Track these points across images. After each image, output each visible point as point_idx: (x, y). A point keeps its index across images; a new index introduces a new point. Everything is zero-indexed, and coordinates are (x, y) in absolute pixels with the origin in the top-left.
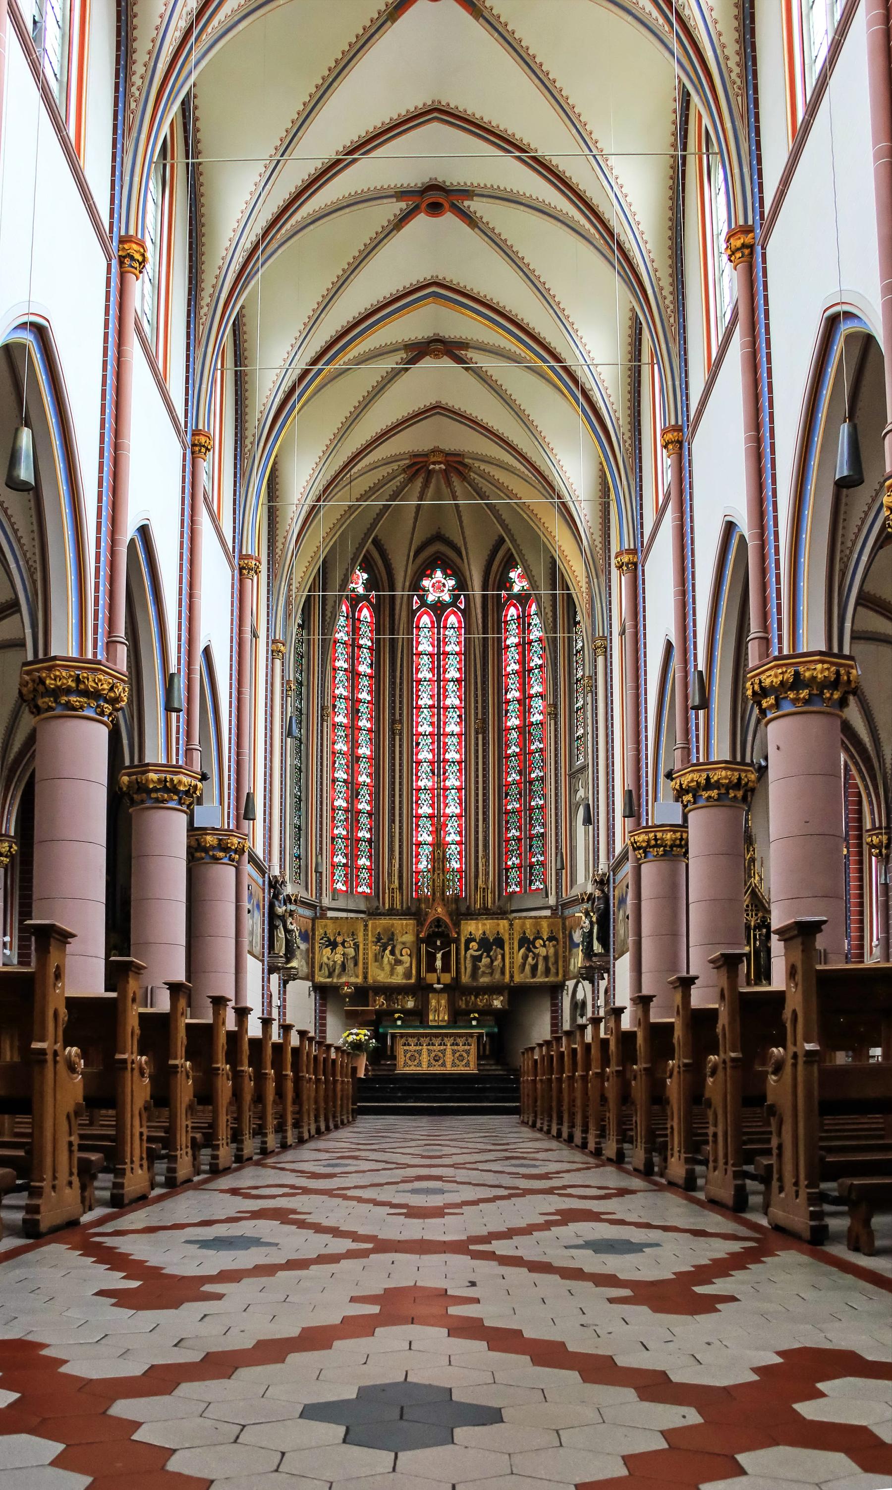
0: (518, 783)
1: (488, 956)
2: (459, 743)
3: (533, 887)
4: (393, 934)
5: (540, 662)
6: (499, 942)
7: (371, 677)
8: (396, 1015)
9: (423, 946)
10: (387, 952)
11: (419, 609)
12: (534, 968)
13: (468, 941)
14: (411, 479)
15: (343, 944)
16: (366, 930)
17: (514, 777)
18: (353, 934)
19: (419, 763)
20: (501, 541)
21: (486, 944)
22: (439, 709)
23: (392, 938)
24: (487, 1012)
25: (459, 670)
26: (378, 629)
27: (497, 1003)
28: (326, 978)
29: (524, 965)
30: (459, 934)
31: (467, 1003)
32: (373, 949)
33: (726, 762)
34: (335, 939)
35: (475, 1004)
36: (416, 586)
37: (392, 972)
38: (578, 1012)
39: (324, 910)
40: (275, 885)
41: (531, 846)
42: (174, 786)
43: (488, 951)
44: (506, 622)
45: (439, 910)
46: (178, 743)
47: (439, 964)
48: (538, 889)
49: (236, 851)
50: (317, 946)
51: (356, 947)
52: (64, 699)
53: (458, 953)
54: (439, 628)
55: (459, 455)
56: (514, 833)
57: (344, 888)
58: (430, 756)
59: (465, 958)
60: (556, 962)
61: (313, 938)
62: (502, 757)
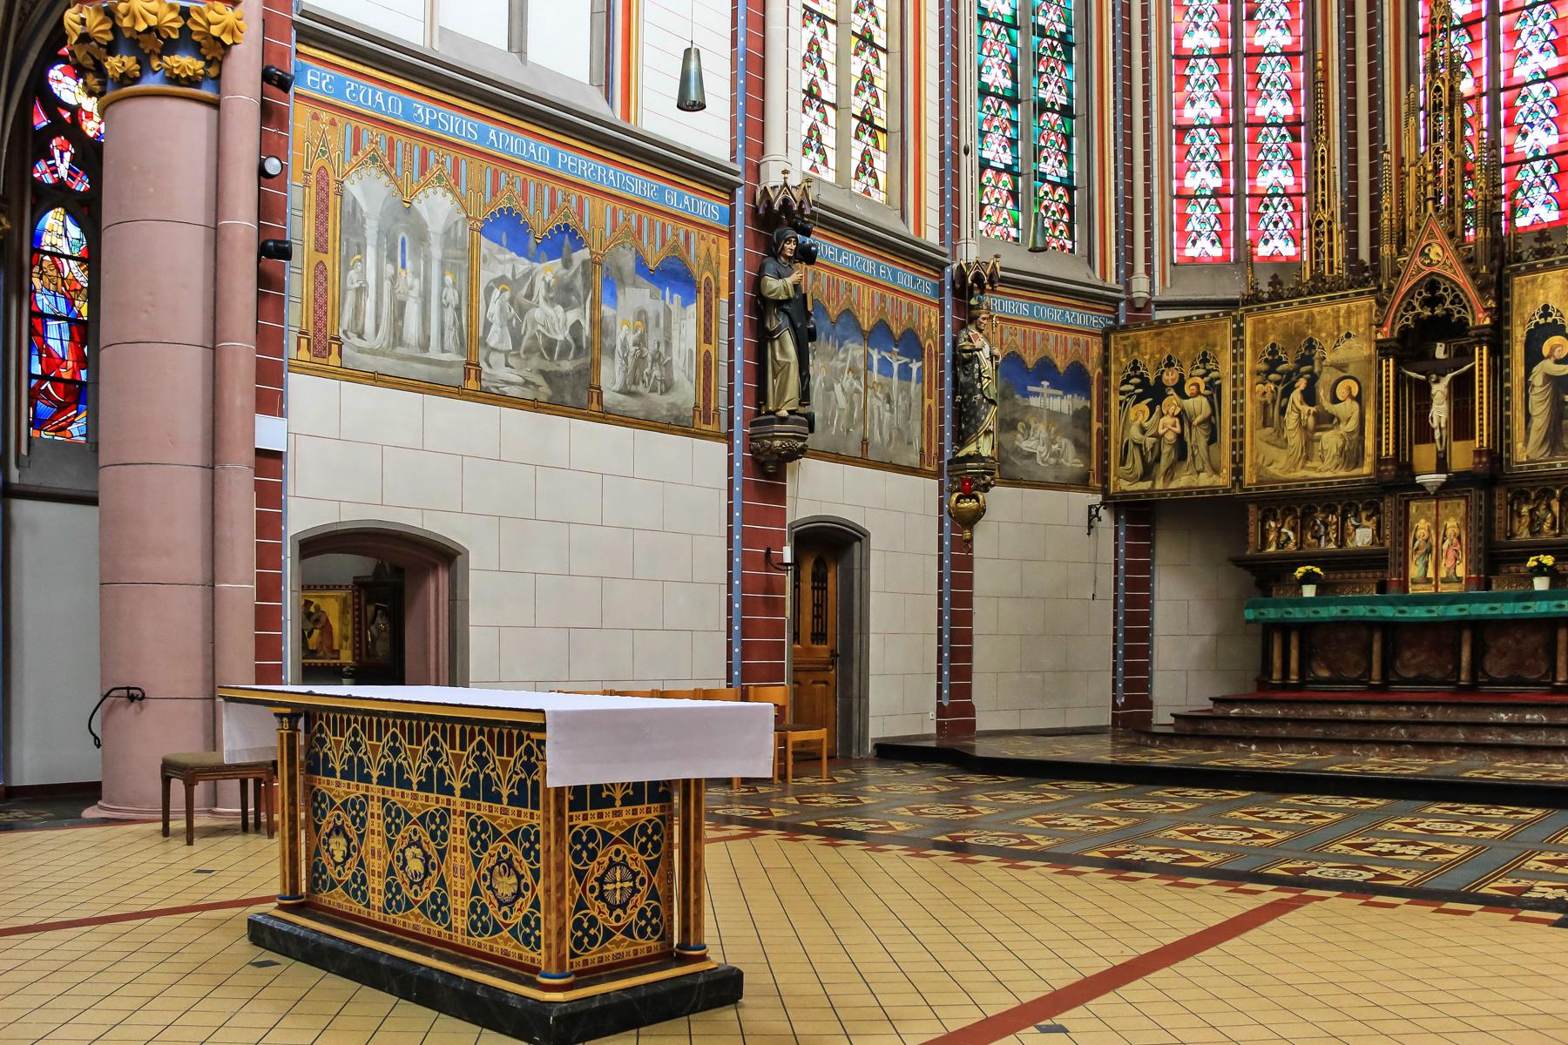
4: (1311, 345)
8: (1300, 572)
10: (1296, 396)
15: (1179, 388)
16: (1238, 343)
18: (1205, 361)
28: (1133, 481)
32: (1256, 391)
34: (1159, 379)
39: (1139, 312)
47: (1439, 412)
50: (1114, 400)
51: (1214, 389)
57: (1217, 251)
59: (1527, 385)
61: (1104, 383)
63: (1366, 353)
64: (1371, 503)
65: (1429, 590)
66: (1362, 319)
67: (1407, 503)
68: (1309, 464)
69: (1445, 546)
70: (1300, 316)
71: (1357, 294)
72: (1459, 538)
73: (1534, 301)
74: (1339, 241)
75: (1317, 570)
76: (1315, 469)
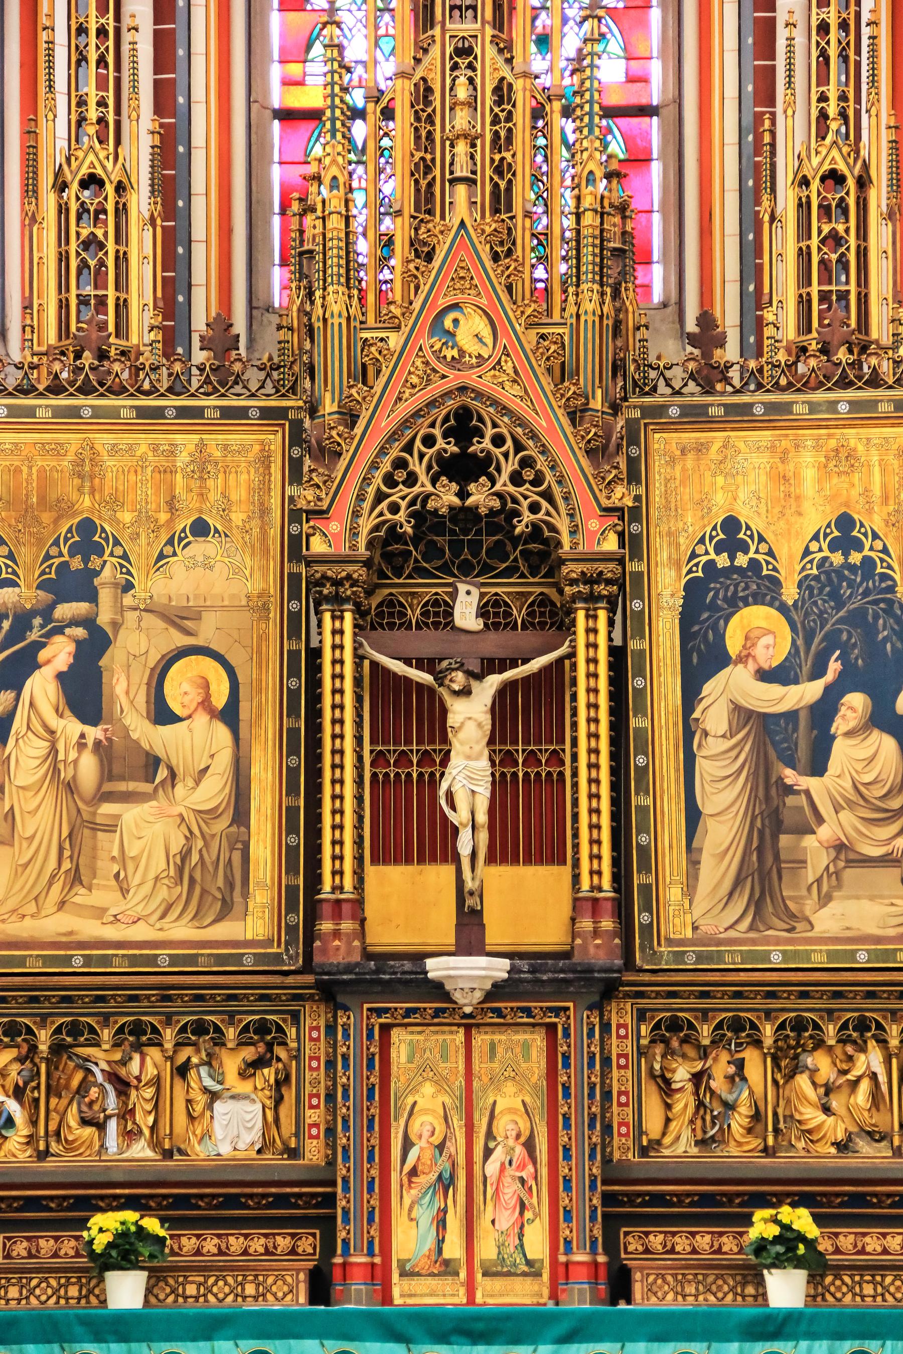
4: (88, 540)
8: (105, 1226)
10: (42, 687)
13: (706, 606)
30: (630, 521)
31: (710, 1111)
45: (471, 330)
47: (468, 779)
59: (689, 731)
63: (254, 586)
64: (262, 1028)
65: (447, 1295)
66: (240, 484)
67: (386, 1029)
68: (81, 896)
69: (492, 1168)
70: (58, 450)
71: (227, 413)
72: (530, 1145)
73: (703, 504)
74: (142, 244)
75: (152, 1225)
76: (99, 912)
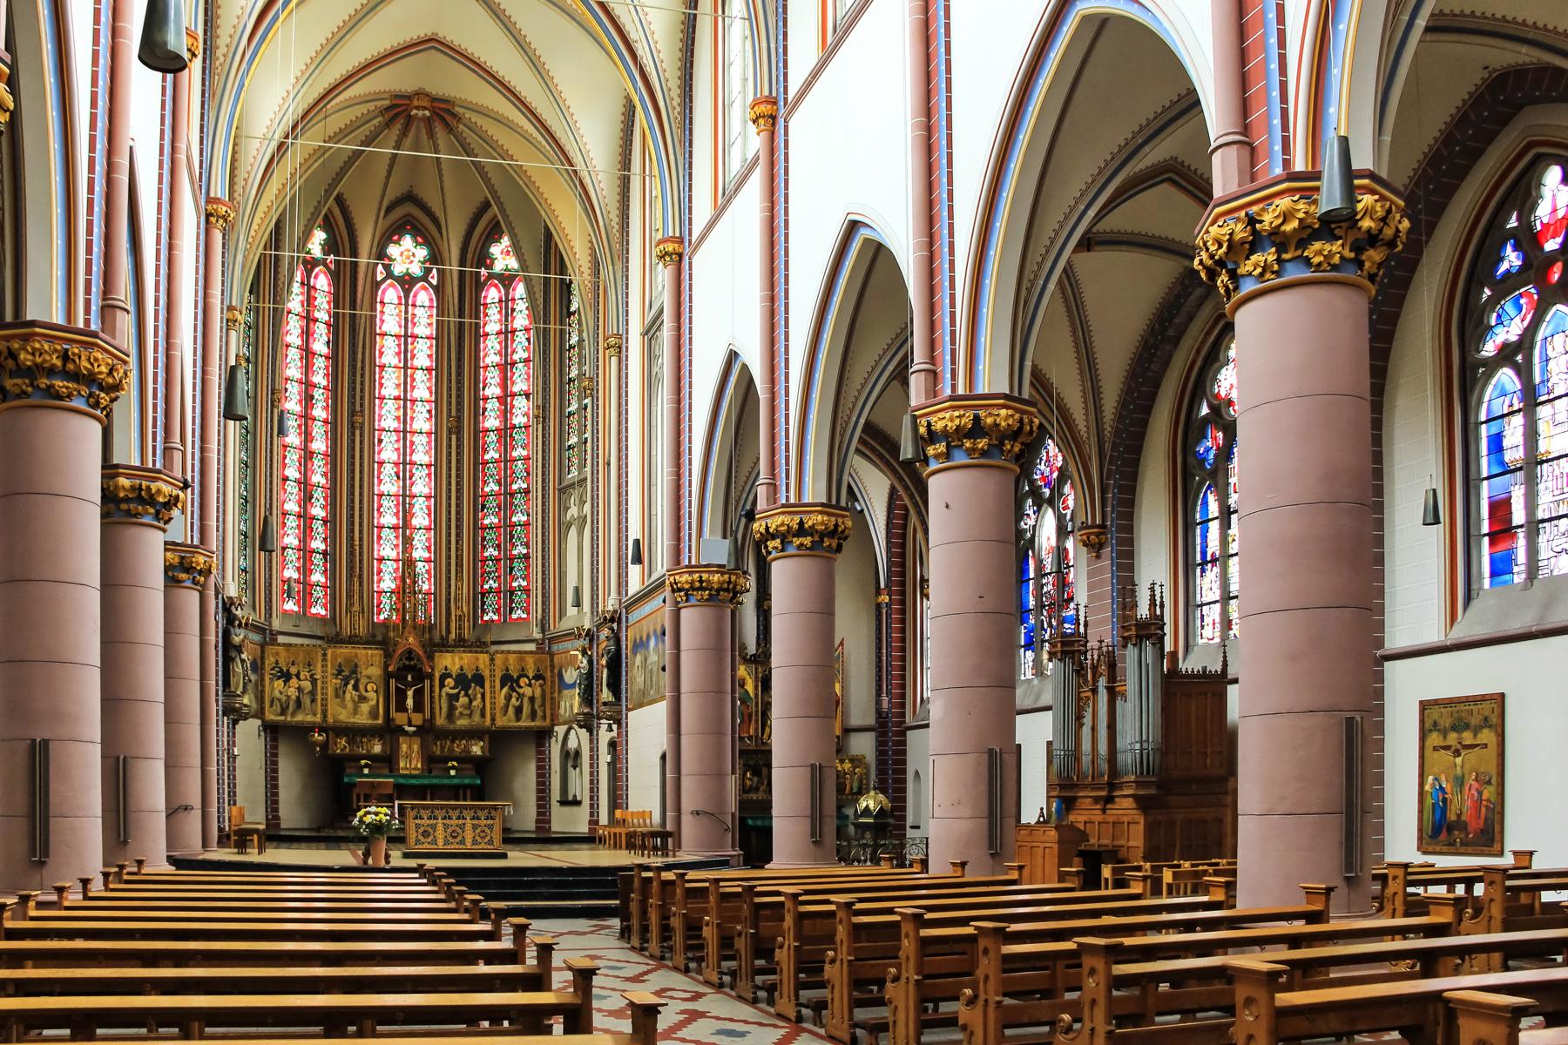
0: (498, 494)
1: (467, 695)
2: (429, 443)
3: (514, 616)
5: (525, 355)
6: (479, 679)
7: (327, 358)
9: (393, 682)
11: (384, 280)
12: (519, 710)
13: (443, 677)
14: (388, 124)
17: (492, 487)
19: (381, 463)
20: (486, 206)
21: (463, 681)
22: (405, 401)
23: (354, 670)
24: (466, 759)
25: (430, 356)
26: (336, 300)
27: (476, 750)
29: (507, 706)
31: (442, 748)
33: (822, 505)
35: (451, 749)
36: (381, 255)
37: (355, 712)
38: (570, 764)
40: (227, 607)
41: (512, 569)
42: (152, 496)
43: (466, 688)
44: (485, 305)
45: (411, 640)
46: (154, 440)
47: (410, 702)
48: (520, 618)
49: (200, 572)
52: (44, 382)
53: (432, 691)
54: (407, 305)
55: (447, 101)
56: (491, 552)
58: (394, 457)
60: (543, 704)
62: (478, 463)
